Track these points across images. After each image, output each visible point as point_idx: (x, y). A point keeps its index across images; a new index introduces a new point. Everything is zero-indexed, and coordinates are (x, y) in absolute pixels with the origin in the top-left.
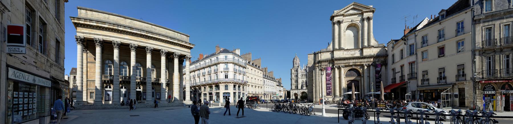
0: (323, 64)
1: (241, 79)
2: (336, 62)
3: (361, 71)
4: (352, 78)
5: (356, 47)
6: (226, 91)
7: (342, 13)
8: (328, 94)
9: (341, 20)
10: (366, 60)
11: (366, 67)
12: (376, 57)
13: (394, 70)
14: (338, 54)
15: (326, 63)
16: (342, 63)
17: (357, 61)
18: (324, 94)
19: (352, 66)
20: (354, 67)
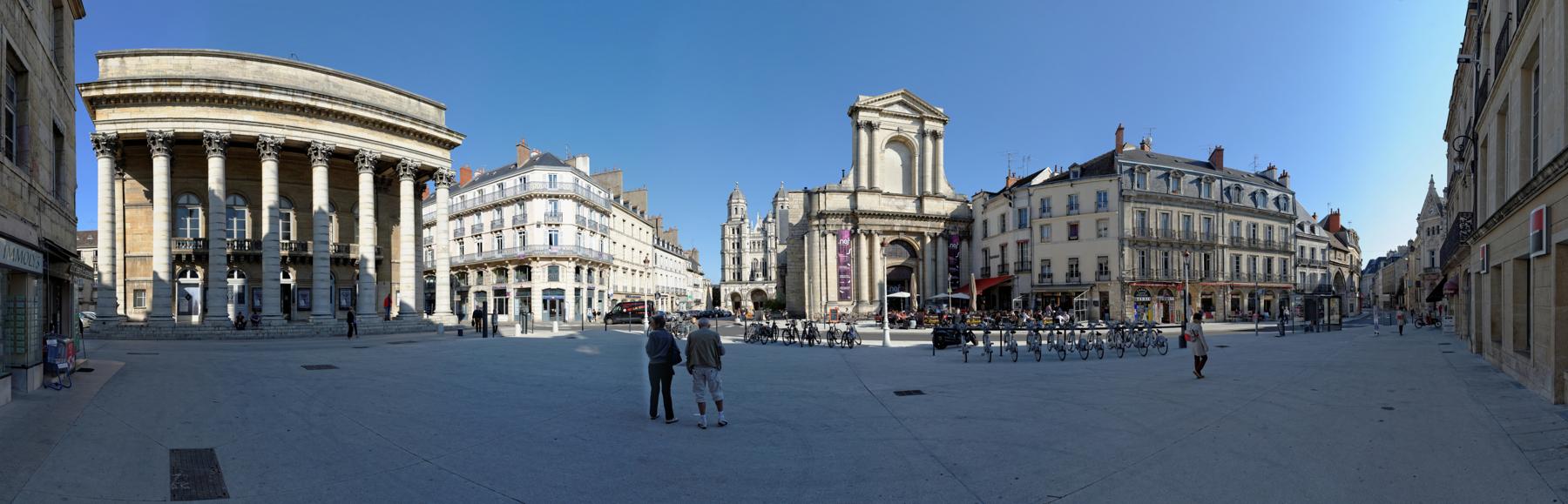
0: (831, 220)
1: (596, 248)
2: (861, 220)
3: (917, 246)
4: (899, 262)
5: (908, 192)
6: (554, 285)
7: (877, 105)
8: (843, 297)
9: (874, 122)
10: (929, 224)
11: (929, 240)
12: (952, 220)
13: (986, 251)
14: (866, 202)
15: (839, 221)
16: (876, 224)
17: (909, 222)
18: (834, 296)
19: (898, 233)
20: (902, 237)
